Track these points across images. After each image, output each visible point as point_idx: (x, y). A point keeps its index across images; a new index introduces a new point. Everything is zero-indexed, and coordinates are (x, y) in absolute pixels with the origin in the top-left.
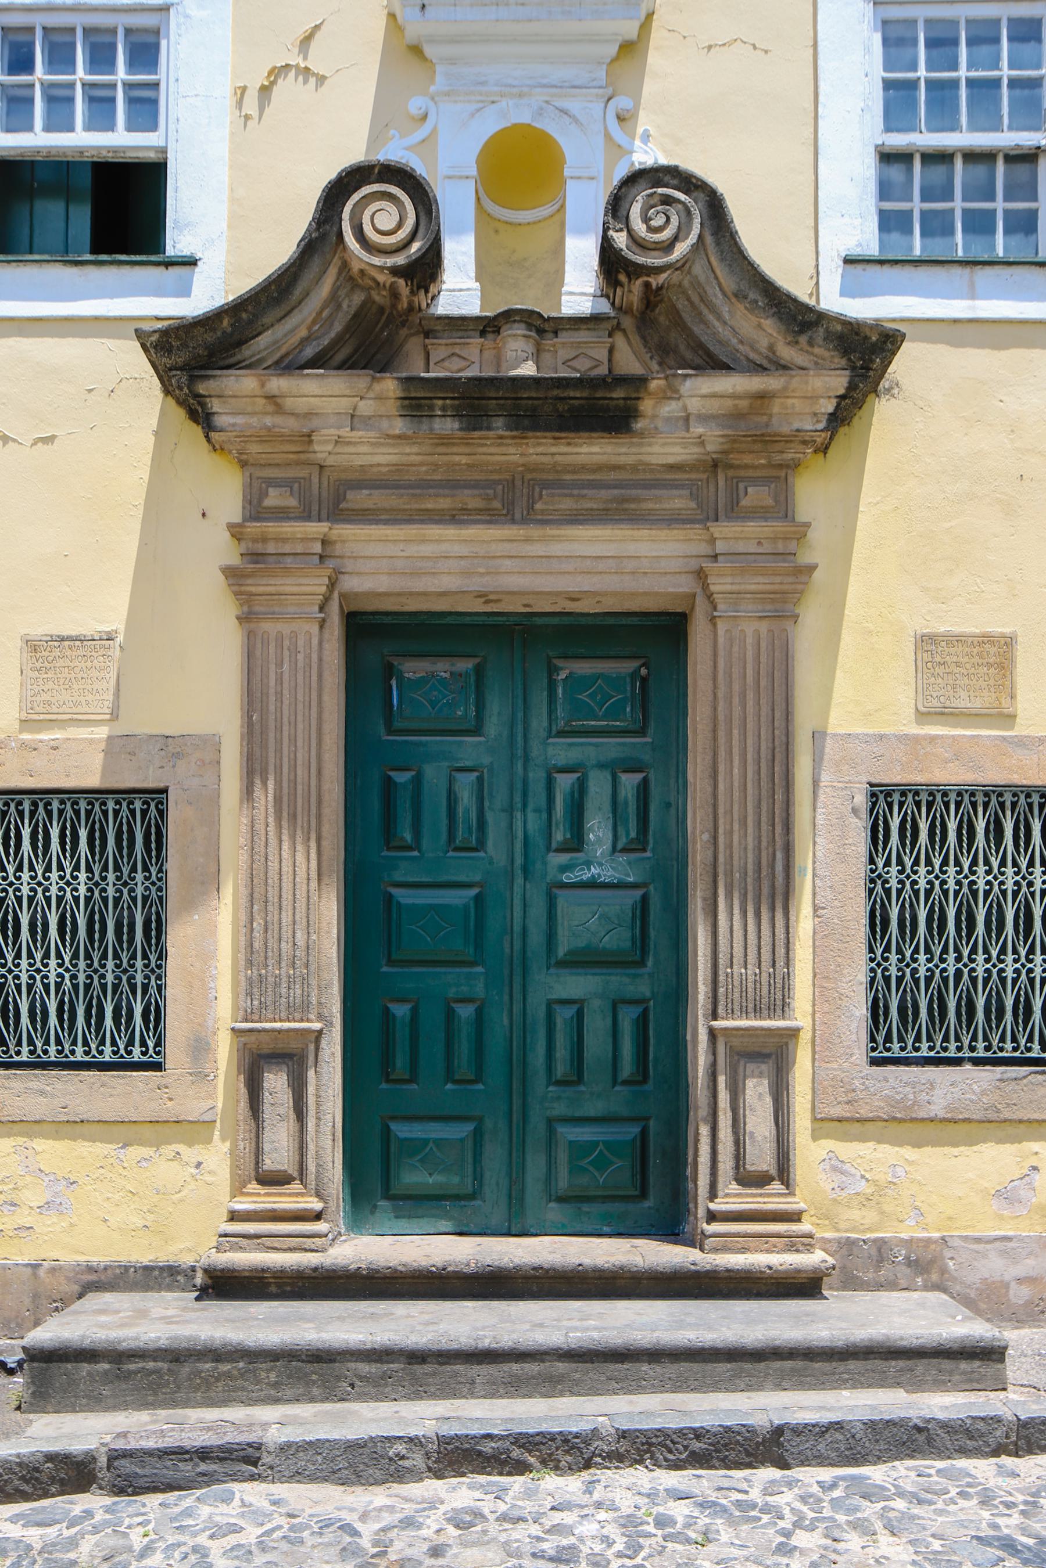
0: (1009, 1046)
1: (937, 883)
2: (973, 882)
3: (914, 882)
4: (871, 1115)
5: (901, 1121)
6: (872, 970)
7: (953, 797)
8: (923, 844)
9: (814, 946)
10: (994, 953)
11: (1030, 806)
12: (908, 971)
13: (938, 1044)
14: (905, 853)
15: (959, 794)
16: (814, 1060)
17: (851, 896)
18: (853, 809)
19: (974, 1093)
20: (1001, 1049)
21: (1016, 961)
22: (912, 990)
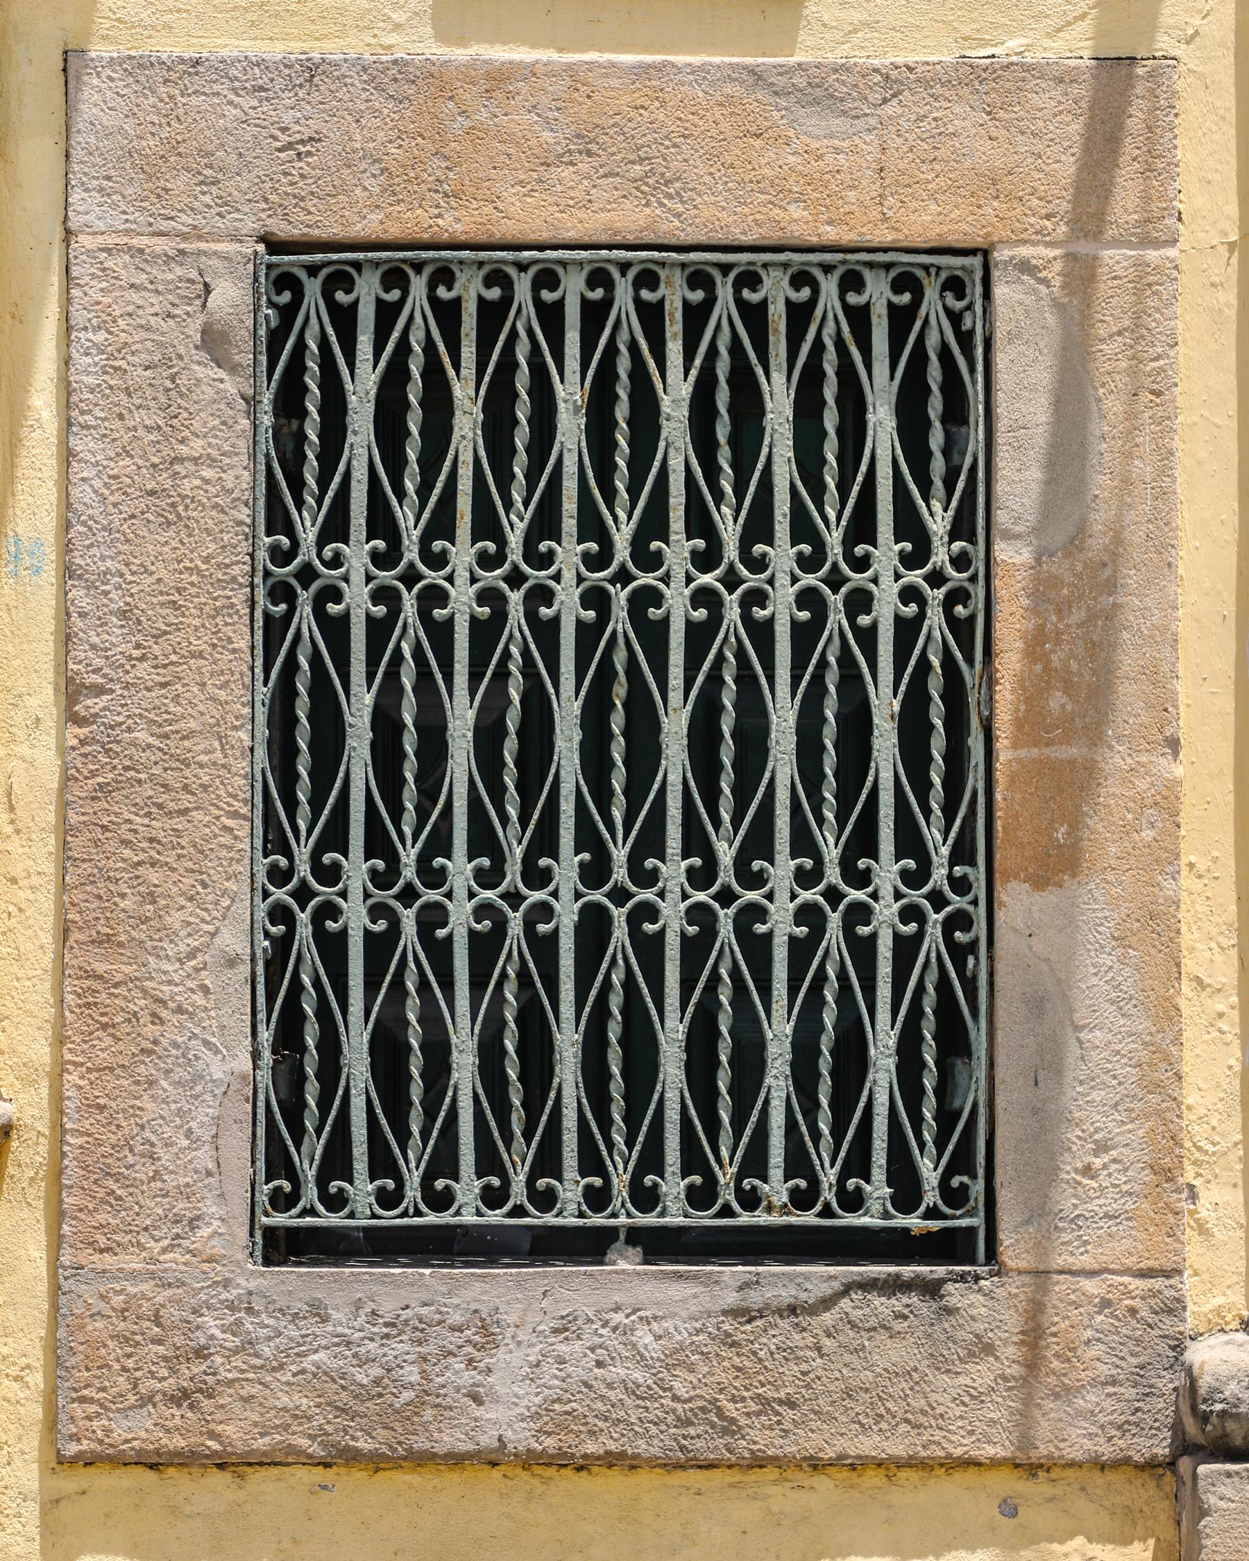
0: (777, 1188)
1: (515, 598)
2: (649, 597)
3: (434, 597)
4: (262, 1443)
5: (377, 1462)
6: (280, 914)
7: (573, 288)
8: (466, 457)
9: (65, 830)
10: (726, 853)
11: (859, 318)
12: (408, 919)
13: (519, 1181)
14: (401, 494)
15: (598, 277)
16: (56, 1242)
17: (199, 645)
18: (206, 331)
19: (640, 1359)
20: (750, 1201)
21: (806, 878)
22: (423, 986)
